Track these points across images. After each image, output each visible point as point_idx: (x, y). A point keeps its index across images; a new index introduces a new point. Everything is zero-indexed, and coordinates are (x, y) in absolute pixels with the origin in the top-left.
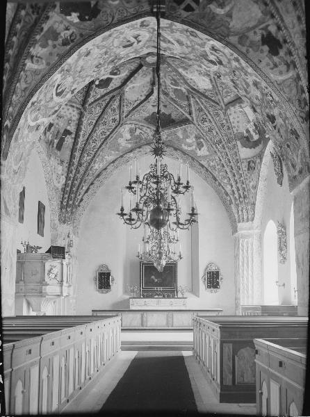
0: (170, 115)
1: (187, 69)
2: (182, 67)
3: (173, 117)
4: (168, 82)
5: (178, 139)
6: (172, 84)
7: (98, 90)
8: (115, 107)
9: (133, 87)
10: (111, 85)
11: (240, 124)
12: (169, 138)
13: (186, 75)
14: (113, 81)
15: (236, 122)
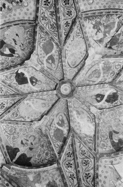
0: (30, 158)
1: (79, 114)
2: (77, 111)
3: (32, 161)
4: (56, 121)
5: (27, 180)
6: (58, 123)
7: (13, 78)
8: (6, 106)
9: (30, 106)
10: (22, 86)
11: (107, 181)
12: (17, 176)
13: (76, 118)
14: (26, 85)
15: (103, 176)
